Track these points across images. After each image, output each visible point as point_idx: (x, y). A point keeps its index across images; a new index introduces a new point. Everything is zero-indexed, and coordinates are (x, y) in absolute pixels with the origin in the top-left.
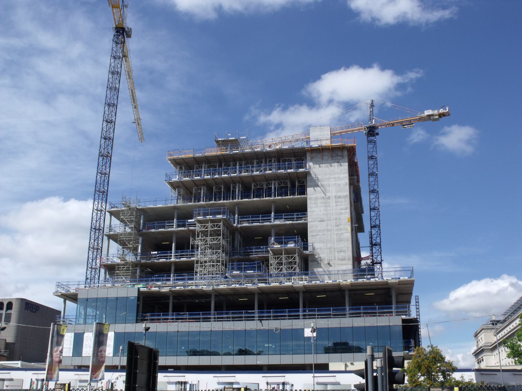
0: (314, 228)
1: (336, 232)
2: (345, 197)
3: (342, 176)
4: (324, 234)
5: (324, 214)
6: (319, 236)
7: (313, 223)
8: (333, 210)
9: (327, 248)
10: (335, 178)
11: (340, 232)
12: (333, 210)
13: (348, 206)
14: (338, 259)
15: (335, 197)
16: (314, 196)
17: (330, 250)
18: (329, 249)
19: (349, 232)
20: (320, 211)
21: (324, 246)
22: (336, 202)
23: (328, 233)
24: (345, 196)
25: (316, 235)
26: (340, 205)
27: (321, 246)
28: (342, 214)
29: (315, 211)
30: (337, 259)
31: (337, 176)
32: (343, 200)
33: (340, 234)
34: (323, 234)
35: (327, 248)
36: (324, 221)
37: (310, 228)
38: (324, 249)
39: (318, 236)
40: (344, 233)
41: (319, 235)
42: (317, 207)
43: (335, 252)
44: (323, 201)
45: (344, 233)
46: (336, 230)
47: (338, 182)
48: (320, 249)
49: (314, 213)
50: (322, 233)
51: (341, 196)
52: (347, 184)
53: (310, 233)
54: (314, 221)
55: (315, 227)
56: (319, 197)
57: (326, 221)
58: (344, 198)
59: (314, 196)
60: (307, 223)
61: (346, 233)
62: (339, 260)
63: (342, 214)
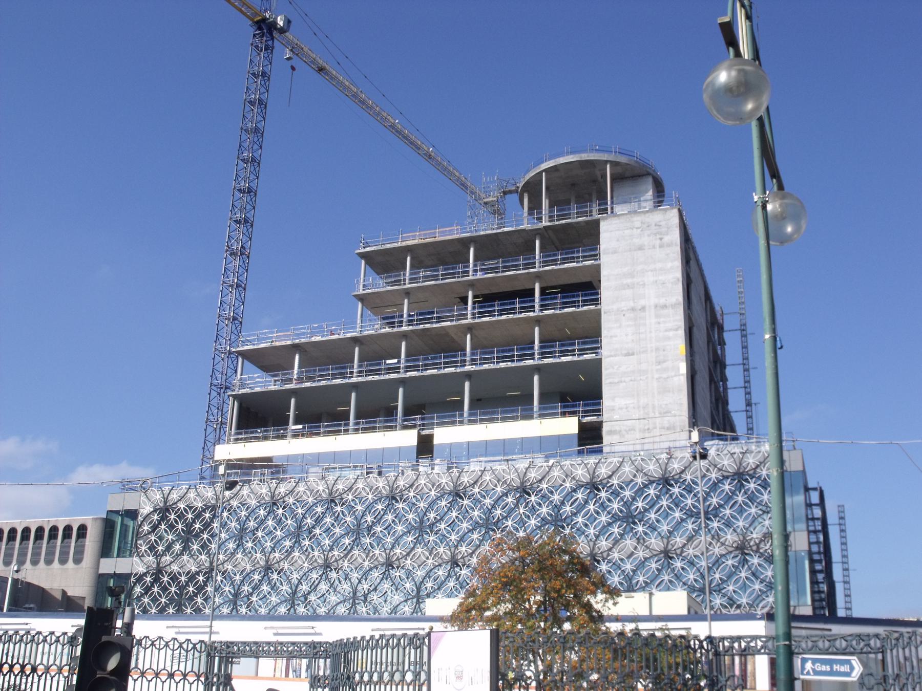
0: (613, 368)
1: (656, 376)
2: (673, 306)
3: (669, 265)
5: (633, 340)
6: (624, 384)
7: (612, 358)
8: (651, 332)
9: (639, 407)
10: (655, 270)
11: (665, 376)
12: (651, 332)
13: (680, 324)
14: (660, 428)
15: (656, 306)
16: (615, 307)
17: (646, 411)
18: (644, 408)
19: (682, 375)
20: (627, 335)
21: (633, 403)
22: (657, 316)
23: (642, 378)
24: (675, 304)
25: (618, 382)
26: (665, 322)
27: (628, 402)
28: (669, 338)
29: (616, 336)
30: (658, 428)
31: (659, 265)
32: (670, 311)
33: (664, 378)
34: (631, 380)
36: (633, 354)
37: (606, 369)
38: (634, 408)
40: (672, 377)
41: (624, 382)
42: (620, 327)
44: (632, 315)
45: (672, 377)
46: (657, 370)
47: (660, 278)
48: (627, 408)
49: (614, 339)
50: (630, 378)
51: (668, 305)
52: (678, 280)
53: (606, 379)
54: (615, 356)
55: (617, 366)
56: (625, 309)
57: (637, 354)
58: (672, 308)
59: (615, 307)
60: (601, 359)
61: (675, 376)
63: (669, 338)
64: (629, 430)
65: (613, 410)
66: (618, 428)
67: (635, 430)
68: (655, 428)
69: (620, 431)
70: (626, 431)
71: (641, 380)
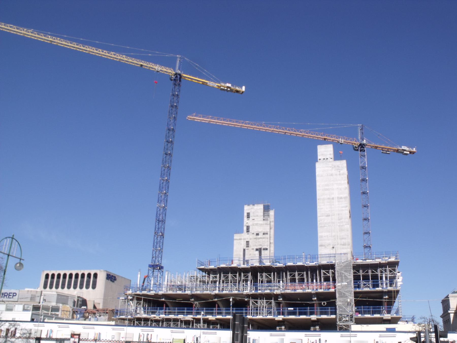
1: (338, 224)
4: (330, 226)
9: (332, 236)
11: (342, 224)
14: (340, 245)
18: (334, 236)
21: (330, 235)
25: (324, 227)
30: (339, 244)
34: (329, 226)
35: (332, 236)
39: (326, 227)
40: (344, 225)
41: (326, 226)
43: (338, 239)
45: (344, 225)
48: (327, 236)
61: (346, 225)
62: (341, 245)
64: (328, 245)
65: (322, 237)
66: (324, 244)
67: (330, 245)
68: (338, 244)
69: (325, 245)
70: (327, 245)
71: (332, 226)
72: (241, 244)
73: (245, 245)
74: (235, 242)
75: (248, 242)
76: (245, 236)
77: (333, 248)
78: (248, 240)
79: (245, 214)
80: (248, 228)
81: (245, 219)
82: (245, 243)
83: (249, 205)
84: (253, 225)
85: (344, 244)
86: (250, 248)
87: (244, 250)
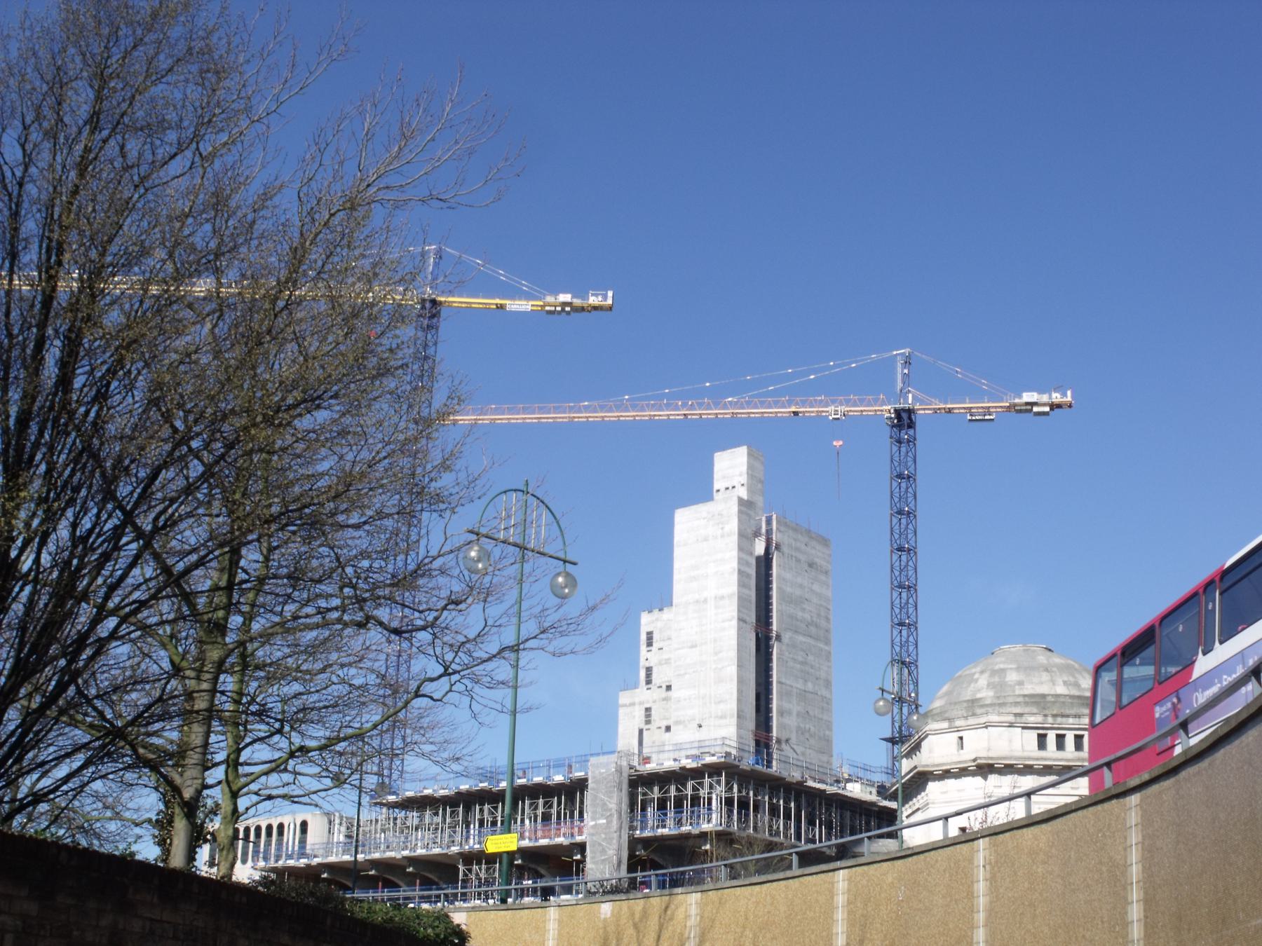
72: (634, 717)
73: (643, 719)
74: (622, 711)
75: (648, 710)
76: (643, 695)
77: (700, 726)
78: (648, 706)
79: (643, 637)
80: (649, 670)
81: (643, 648)
82: (643, 712)
83: (650, 611)
84: (660, 664)
85: (723, 717)
86: (653, 726)
87: (641, 732)
